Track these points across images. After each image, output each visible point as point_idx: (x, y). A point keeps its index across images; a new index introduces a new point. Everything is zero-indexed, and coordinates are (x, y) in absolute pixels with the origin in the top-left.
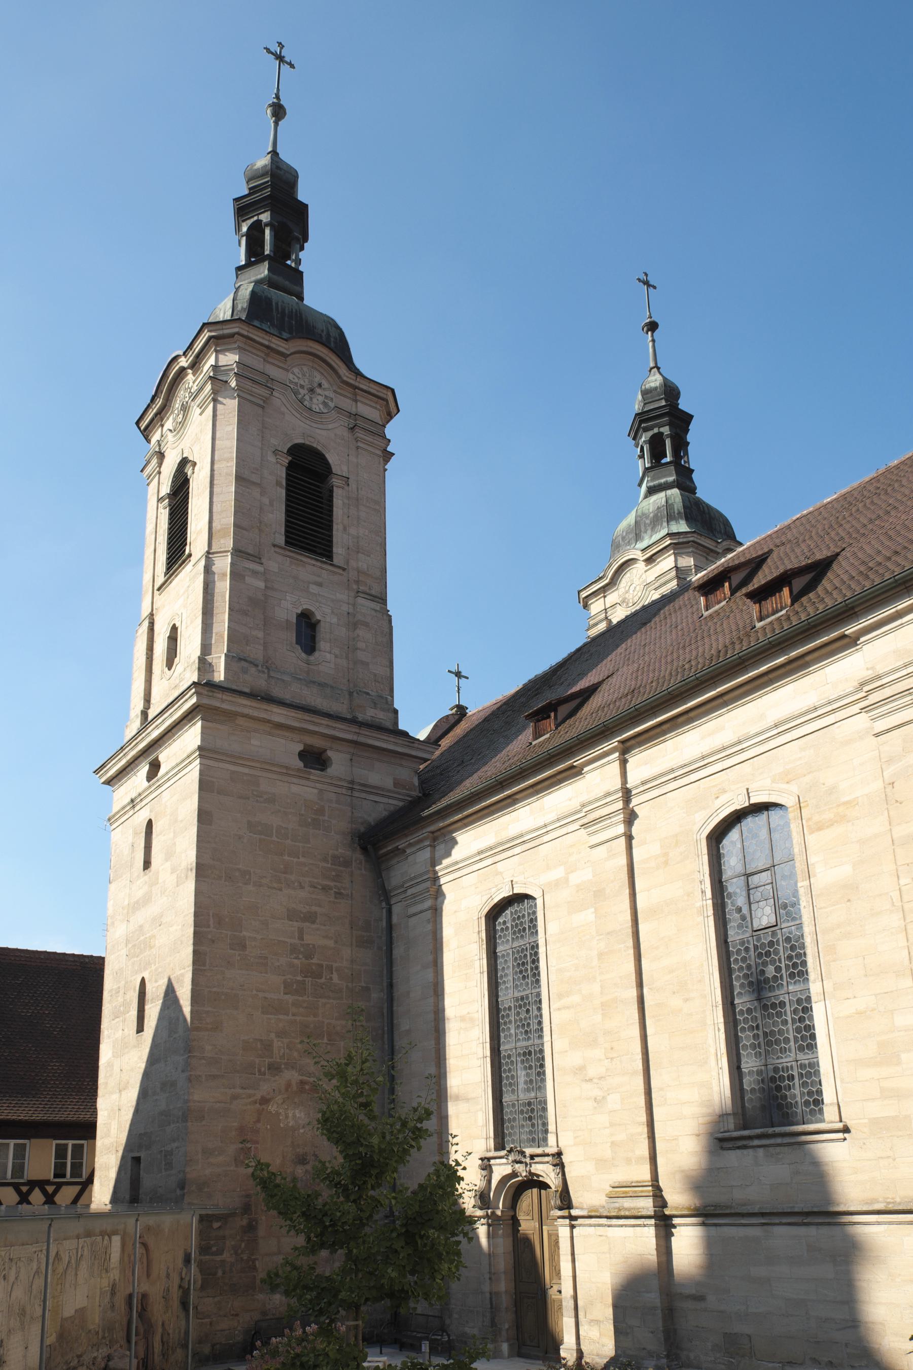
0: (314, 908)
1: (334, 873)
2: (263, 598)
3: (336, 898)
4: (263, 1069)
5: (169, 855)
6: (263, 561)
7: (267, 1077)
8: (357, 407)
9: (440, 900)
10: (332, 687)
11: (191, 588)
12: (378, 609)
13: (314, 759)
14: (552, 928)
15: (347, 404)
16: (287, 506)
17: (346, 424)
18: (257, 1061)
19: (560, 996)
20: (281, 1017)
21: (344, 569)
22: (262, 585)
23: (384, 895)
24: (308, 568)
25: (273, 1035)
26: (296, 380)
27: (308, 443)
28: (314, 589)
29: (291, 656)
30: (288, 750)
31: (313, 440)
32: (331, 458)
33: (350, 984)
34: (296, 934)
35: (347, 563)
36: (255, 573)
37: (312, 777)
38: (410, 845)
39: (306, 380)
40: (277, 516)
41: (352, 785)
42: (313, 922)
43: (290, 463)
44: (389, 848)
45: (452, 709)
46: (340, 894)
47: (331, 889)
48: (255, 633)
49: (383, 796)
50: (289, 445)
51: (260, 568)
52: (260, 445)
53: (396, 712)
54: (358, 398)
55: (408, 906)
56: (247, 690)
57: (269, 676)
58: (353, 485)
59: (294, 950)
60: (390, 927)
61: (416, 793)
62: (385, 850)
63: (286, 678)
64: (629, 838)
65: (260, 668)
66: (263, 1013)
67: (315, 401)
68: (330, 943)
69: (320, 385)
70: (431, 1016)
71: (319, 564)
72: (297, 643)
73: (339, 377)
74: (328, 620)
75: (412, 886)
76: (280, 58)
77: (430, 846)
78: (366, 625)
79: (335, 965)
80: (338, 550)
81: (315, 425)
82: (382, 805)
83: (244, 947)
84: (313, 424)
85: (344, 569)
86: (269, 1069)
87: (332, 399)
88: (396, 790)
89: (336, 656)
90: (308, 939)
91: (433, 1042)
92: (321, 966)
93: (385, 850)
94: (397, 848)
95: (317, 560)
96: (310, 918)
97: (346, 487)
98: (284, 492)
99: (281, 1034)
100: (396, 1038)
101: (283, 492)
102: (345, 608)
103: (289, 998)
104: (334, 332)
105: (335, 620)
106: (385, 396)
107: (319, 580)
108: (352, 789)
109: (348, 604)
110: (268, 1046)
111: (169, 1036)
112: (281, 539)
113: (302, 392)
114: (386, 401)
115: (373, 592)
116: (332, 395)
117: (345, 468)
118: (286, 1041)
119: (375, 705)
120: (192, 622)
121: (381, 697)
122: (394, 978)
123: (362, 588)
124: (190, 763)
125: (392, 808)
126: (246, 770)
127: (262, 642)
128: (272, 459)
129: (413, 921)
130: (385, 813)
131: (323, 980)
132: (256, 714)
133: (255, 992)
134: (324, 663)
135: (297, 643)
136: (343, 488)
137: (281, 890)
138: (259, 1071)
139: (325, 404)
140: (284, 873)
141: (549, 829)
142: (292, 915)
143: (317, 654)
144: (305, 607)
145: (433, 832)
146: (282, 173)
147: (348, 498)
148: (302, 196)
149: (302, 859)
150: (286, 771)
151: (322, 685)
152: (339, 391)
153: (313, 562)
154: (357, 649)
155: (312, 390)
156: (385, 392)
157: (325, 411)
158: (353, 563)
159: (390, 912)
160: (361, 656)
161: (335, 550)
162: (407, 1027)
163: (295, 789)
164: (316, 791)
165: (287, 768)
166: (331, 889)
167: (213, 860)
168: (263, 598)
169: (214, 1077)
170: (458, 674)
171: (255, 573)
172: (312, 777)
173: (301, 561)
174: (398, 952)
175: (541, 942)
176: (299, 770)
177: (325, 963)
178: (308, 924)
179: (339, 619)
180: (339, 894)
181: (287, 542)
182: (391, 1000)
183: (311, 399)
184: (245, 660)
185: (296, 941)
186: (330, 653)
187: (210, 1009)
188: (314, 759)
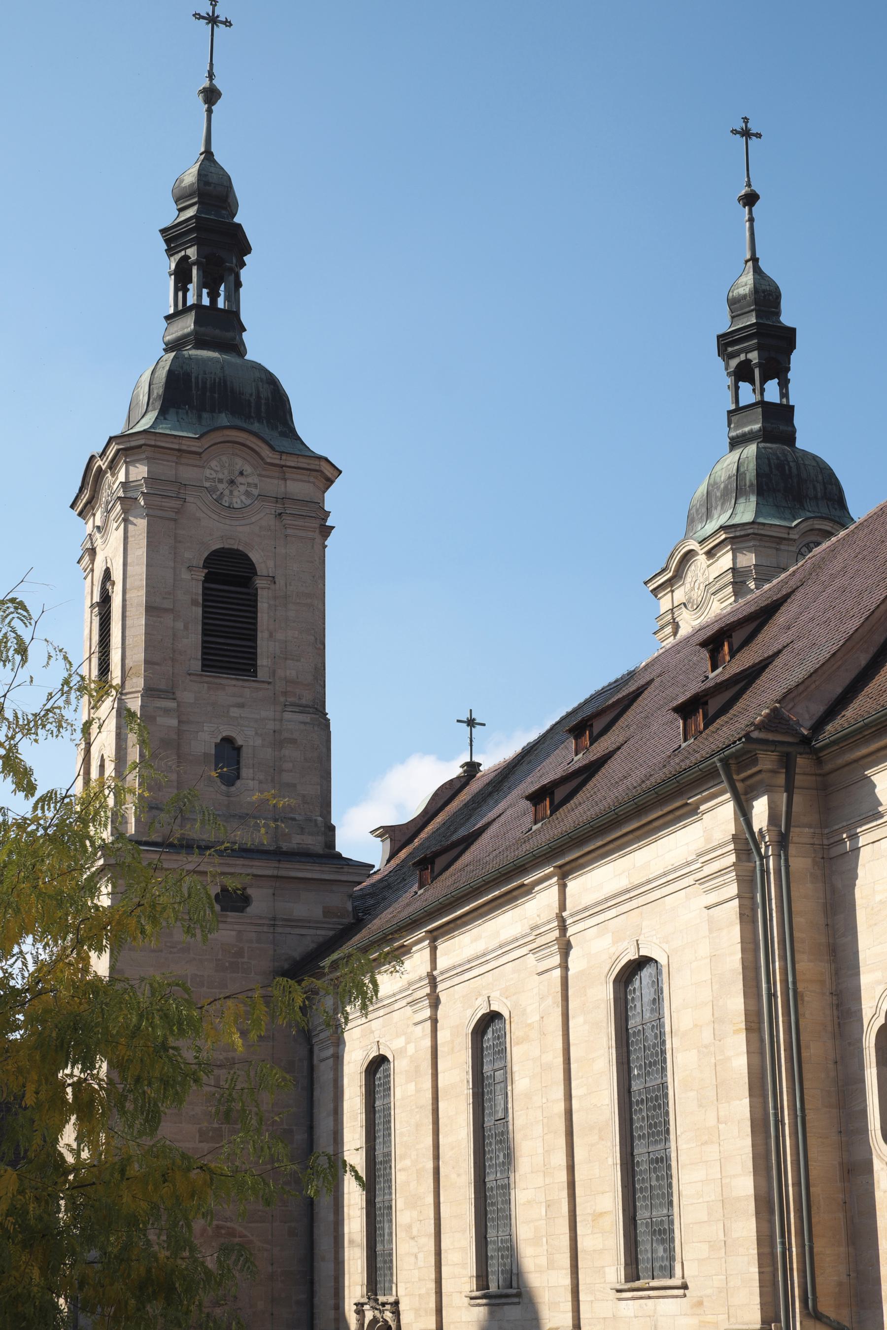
6: (178, 694)
8: (286, 487)
9: (341, 1047)
12: (308, 720)
15: (273, 486)
21: (269, 683)
24: (230, 689)
26: (214, 475)
27: (227, 546)
28: (235, 712)
29: (209, 791)
36: (167, 711)
37: (229, 920)
39: (226, 472)
45: (462, 766)
49: (309, 927)
50: (206, 554)
51: (172, 705)
52: (172, 564)
58: (280, 581)
61: (350, 920)
64: (434, 1021)
67: (236, 493)
69: (241, 473)
71: (240, 683)
73: (262, 459)
78: (293, 741)
80: (263, 661)
81: (237, 523)
85: (269, 683)
87: (256, 486)
89: (261, 782)
95: (238, 679)
97: (273, 586)
98: (199, 610)
102: (271, 726)
105: (259, 742)
106: (317, 468)
108: (274, 925)
109: (275, 720)
112: (197, 665)
113: (221, 486)
115: (304, 702)
117: (271, 564)
119: (302, 831)
123: (291, 699)
125: (321, 939)
127: (175, 784)
128: (185, 575)
130: (312, 946)
136: (269, 588)
139: (248, 494)
141: (397, 998)
143: (238, 783)
152: (264, 473)
153: (234, 682)
155: (232, 482)
156: (317, 462)
161: (259, 662)
164: (234, 933)
168: (175, 737)
172: (229, 920)
173: (221, 684)
183: (231, 492)
188: (233, 901)
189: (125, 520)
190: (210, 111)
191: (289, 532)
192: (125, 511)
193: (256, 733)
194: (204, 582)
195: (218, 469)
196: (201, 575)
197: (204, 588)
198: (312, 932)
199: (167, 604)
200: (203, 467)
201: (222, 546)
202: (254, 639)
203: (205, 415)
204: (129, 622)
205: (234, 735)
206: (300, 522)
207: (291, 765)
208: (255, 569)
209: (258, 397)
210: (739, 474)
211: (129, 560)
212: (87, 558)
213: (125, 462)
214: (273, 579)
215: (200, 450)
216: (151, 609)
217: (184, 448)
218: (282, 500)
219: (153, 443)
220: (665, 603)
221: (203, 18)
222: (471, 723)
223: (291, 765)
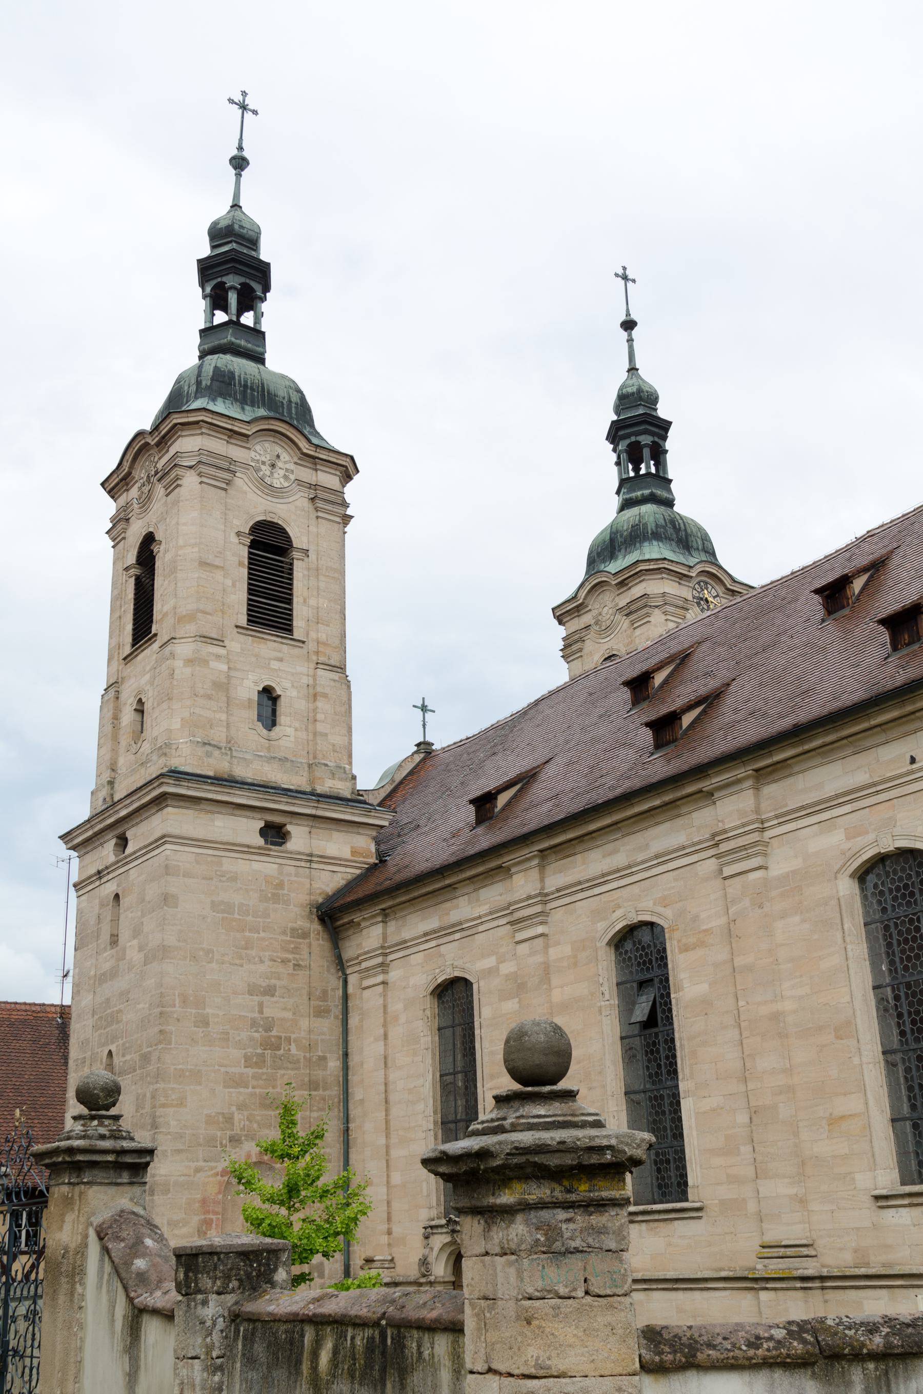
0: (273, 981)
1: (292, 946)
2: (225, 681)
3: (294, 970)
4: (224, 1142)
6: (226, 643)
7: (228, 1149)
10: (292, 761)
11: (157, 671)
13: (275, 833)
15: (307, 474)
17: (306, 495)
18: (219, 1134)
20: (242, 1090)
23: (340, 964)
25: (234, 1109)
26: (258, 457)
27: (269, 519)
28: (275, 665)
30: (248, 830)
31: (273, 515)
33: (308, 1055)
34: (257, 1010)
35: (308, 634)
36: (218, 657)
37: (272, 853)
39: (268, 456)
40: (239, 597)
41: (310, 858)
42: (273, 996)
43: (252, 541)
44: (346, 920)
46: (299, 965)
47: (289, 961)
48: (218, 716)
49: (340, 865)
50: (251, 524)
51: (222, 651)
52: (222, 527)
54: (318, 467)
55: (362, 979)
56: (211, 774)
57: (232, 757)
59: (254, 1024)
60: (346, 997)
61: (373, 860)
62: (341, 922)
63: (248, 756)
65: (223, 750)
66: (225, 1087)
67: (276, 475)
68: (289, 1015)
70: (382, 1088)
72: (258, 720)
73: (299, 449)
74: (288, 693)
75: (365, 960)
76: (244, 107)
77: (383, 922)
78: (325, 696)
79: (293, 1036)
80: (298, 623)
81: (277, 500)
82: (339, 874)
83: (207, 1024)
84: (274, 500)
85: (303, 642)
86: (230, 1141)
88: (353, 858)
89: (296, 730)
90: (267, 1012)
91: (384, 1113)
92: (280, 1038)
93: (341, 922)
94: (352, 921)
95: (278, 636)
96: (270, 991)
97: (306, 559)
98: (246, 571)
99: (241, 1107)
100: (351, 1106)
101: (245, 571)
102: (305, 680)
103: (250, 1071)
104: (295, 398)
106: (344, 463)
107: (279, 655)
108: (311, 861)
110: (229, 1119)
111: (137, 1111)
112: (243, 620)
113: (263, 467)
114: (347, 469)
115: (332, 662)
116: (291, 466)
117: (305, 539)
118: (246, 1113)
120: (158, 705)
121: (340, 767)
122: (349, 1047)
123: (322, 659)
125: (349, 877)
127: (225, 724)
128: (235, 540)
129: (367, 993)
131: (282, 1052)
133: (217, 1067)
134: (284, 738)
135: (258, 720)
137: (242, 966)
138: (221, 1144)
139: (286, 477)
140: (246, 948)
142: (252, 990)
143: (277, 729)
144: (266, 683)
145: (384, 910)
146: (245, 231)
147: (309, 569)
148: (265, 255)
149: (262, 934)
150: (247, 850)
151: (283, 760)
154: (316, 721)
155: (273, 466)
157: (286, 484)
158: (313, 635)
159: (345, 982)
160: (320, 727)
162: (361, 1097)
163: (256, 866)
164: (276, 866)
165: (248, 846)
166: (289, 961)
167: (179, 941)
168: (225, 681)
169: (179, 1151)
170: (424, 708)
172: (272, 853)
173: (263, 638)
174: (353, 1021)
176: (259, 848)
177: (283, 1035)
178: (267, 997)
179: (298, 692)
180: (297, 966)
182: (346, 1068)
183: (272, 473)
184: (210, 744)
185: (256, 1015)
186: (290, 727)
187: (175, 1086)
190: (239, 175)
191: (320, 514)
193: (293, 686)
194: (250, 547)
195: (262, 452)
196: (248, 541)
197: (250, 553)
199: (218, 562)
200: (249, 449)
201: (264, 518)
202: (289, 601)
203: (247, 408)
205: (274, 685)
206: (329, 507)
207: (323, 716)
208: (290, 541)
209: (290, 401)
214: (306, 552)
215: (250, 433)
217: (236, 429)
219: (209, 420)
221: (236, 103)
222: (424, 708)
223: (323, 716)
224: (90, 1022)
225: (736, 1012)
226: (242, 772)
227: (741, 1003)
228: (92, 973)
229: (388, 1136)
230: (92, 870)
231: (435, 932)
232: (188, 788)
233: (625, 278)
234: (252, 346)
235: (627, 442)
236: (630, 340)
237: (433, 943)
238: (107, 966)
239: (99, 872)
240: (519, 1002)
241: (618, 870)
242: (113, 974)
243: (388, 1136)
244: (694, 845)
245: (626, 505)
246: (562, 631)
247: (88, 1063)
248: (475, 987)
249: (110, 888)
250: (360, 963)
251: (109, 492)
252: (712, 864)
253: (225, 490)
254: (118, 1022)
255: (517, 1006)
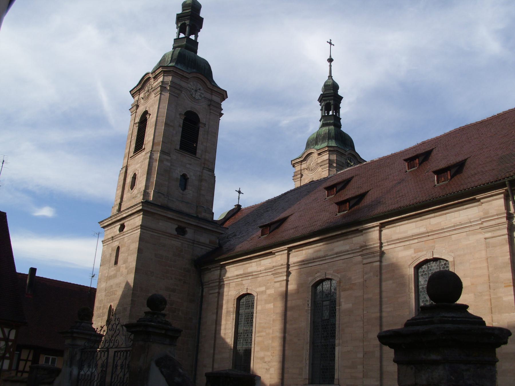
5: (125, 262)
9: (221, 290)
13: (181, 231)
14: (259, 308)
15: (208, 96)
16: (182, 134)
19: (259, 332)
22: (169, 164)
23: (201, 284)
28: (188, 166)
30: (171, 228)
32: (200, 116)
36: (167, 160)
38: (213, 268)
40: (178, 138)
51: (169, 158)
53: (213, 213)
56: (160, 204)
57: (168, 199)
58: (207, 126)
60: (202, 296)
61: (217, 246)
69: (200, 89)
70: (214, 332)
75: (212, 283)
80: (199, 151)
101: (181, 129)
108: (194, 243)
112: (178, 147)
116: (203, 92)
123: (206, 166)
124: (137, 230)
126: (156, 234)
128: (178, 116)
132: (162, 214)
139: (200, 96)
143: (186, 191)
148: (202, 15)
155: (196, 91)
159: (202, 291)
164: (180, 243)
165: (171, 234)
170: (239, 192)
171: (167, 160)
175: (255, 312)
176: (175, 235)
181: (180, 148)
189: (161, 94)
192: (161, 91)
196: (183, 118)
198: (206, 248)
204: (157, 127)
210: (329, 133)
211: (160, 107)
212: (135, 108)
213: (164, 75)
216: (166, 124)
218: (210, 100)
220: (298, 168)
222: (239, 192)
224: (104, 294)
225: (362, 316)
226: (171, 205)
227: (365, 312)
228: (106, 275)
229: (214, 350)
230: (110, 236)
231: (241, 275)
232: (151, 208)
233: (330, 43)
234: (194, 45)
235: (326, 102)
236: (331, 66)
237: (240, 279)
238: (112, 273)
239: (112, 237)
240: (274, 305)
241: (320, 258)
242: (115, 276)
243: (214, 350)
244: (352, 250)
245: (323, 125)
246: (293, 170)
247: (102, 308)
248: (256, 298)
249: (116, 244)
250: (209, 284)
251: (132, 95)
252: (359, 258)
253: (177, 97)
254: (115, 295)
255: (272, 306)
